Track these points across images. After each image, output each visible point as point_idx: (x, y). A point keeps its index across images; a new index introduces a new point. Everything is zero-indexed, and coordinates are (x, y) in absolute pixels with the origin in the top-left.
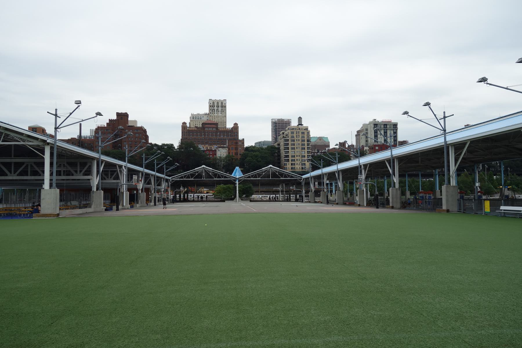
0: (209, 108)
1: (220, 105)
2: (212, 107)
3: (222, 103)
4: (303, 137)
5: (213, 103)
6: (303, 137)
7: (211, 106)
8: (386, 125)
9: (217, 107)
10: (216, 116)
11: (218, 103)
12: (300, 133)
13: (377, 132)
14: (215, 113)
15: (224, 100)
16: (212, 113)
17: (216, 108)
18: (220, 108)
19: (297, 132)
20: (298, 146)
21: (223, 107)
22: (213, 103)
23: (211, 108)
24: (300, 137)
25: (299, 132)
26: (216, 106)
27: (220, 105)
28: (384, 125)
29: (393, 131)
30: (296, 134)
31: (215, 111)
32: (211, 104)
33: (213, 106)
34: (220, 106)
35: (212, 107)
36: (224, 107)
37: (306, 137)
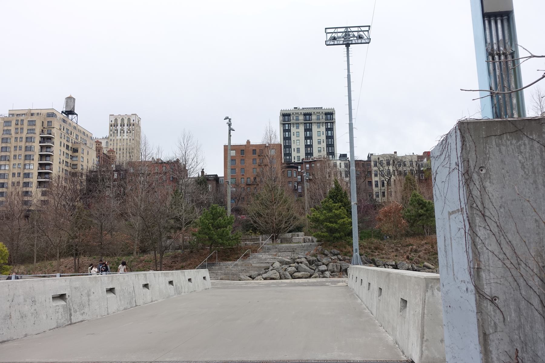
0: (110, 128)
1: (126, 122)
2: (113, 126)
3: (129, 119)
4: (31, 131)
5: (116, 120)
6: (31, 131)
7: (111, 126)
8: (310, 114)
9: (121, 126)
10: (119, 141)
11: (123, 120)
12: (26, 123)
13: (289, 131)
14: (117, 135)
15: (132, 114)
16: (113, 135)
17: (119, 128)
18: (126, 128)
19: (17, 121)
20: (18, 152)
21: (130, 125)
22: (116, 120)
23: (111, 127)
24: (25, 131)
25: (22, 120)
26: (119, 125)
27: (126, 122)
28: (305, 115)
29: (324, 126)
30: (17, 127)
31: (124, 133)
32: (112, 121)
33: (116, 125)
34: (126, 125)
35: (113, 126)
36: (132, 125)
37: (125, 146)
